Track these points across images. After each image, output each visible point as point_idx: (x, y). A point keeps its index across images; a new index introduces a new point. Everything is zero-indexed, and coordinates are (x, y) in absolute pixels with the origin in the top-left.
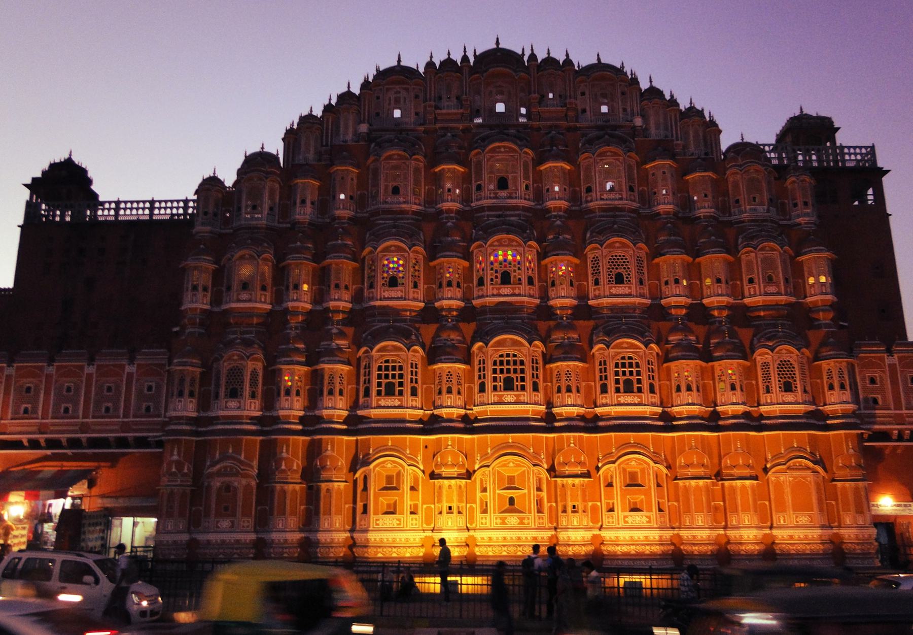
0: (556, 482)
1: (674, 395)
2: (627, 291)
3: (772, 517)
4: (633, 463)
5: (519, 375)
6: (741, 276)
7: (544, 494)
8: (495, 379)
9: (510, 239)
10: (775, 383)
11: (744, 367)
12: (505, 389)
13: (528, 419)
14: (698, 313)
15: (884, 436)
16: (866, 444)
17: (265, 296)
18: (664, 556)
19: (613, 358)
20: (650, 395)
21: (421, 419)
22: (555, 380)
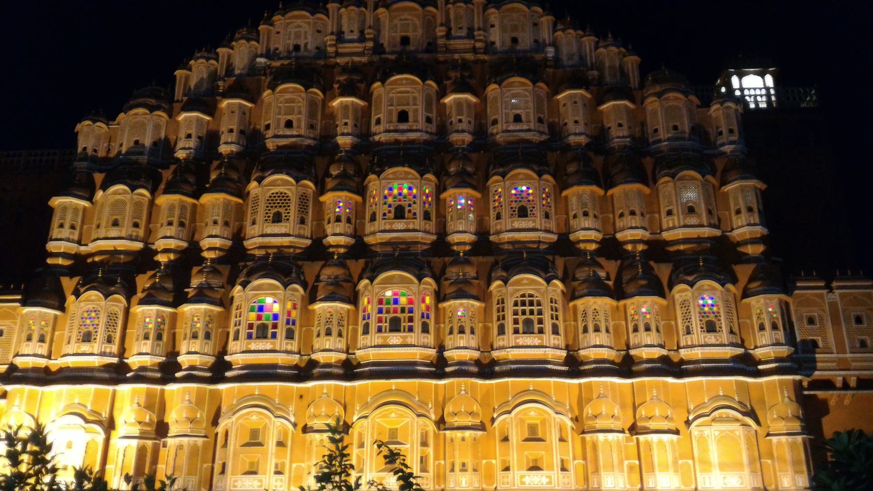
0: (445, 434)
1: (581, 336)
2: (531, 225)
3: (696, 479)
4: (532, 413)
5: (407, 315)
6: (659, 208)
7: (430, 450)
8: (380, 320)
9: (405, 172)
10: (696, 324)
11: (661, 306)
12: (391, 331)
13: (415, 364)
14: (611, 247)
15: (828, 385)
16: (806, 393)
17: (137, 232)
19: (512, 295)
20: (552, 336)
21: (296, 365)
22: (447, 321)
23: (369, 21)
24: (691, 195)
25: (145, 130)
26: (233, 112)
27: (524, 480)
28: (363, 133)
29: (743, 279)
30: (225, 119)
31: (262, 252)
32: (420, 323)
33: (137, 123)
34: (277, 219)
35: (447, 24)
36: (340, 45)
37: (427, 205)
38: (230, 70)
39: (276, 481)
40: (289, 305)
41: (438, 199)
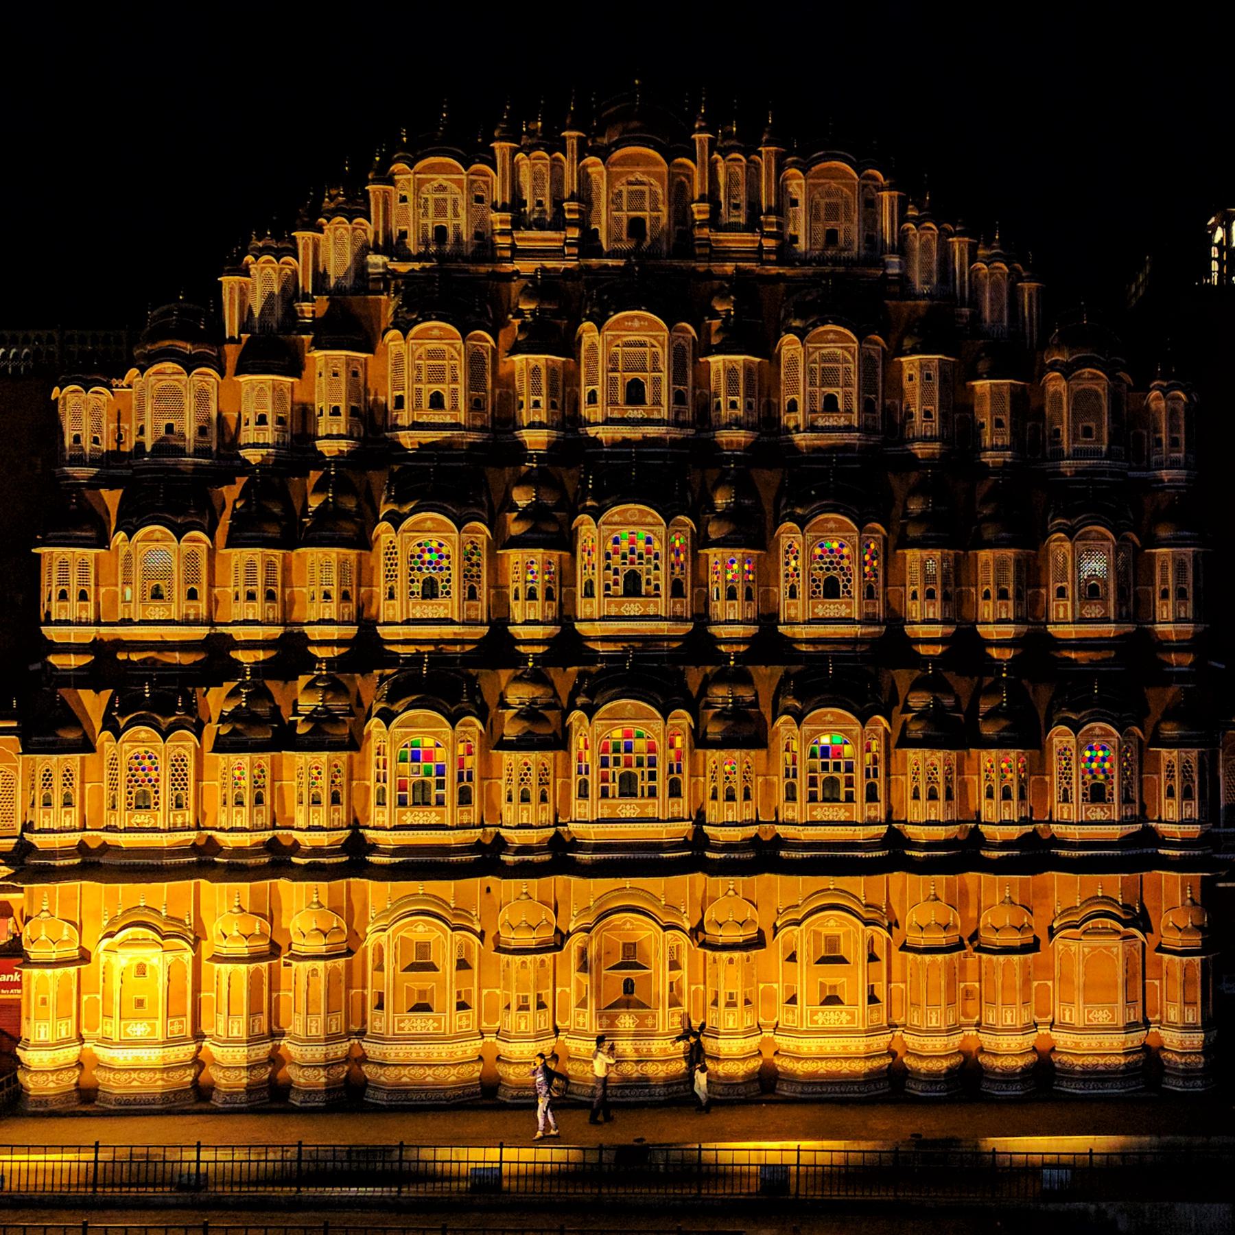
4: (832, 923)
9: (640, 511)
18: (872, 1077)
23: (570, 184)
24: (1096, 566)
25: (182, 404)
26: (335, 374)
27: (815, 1018)
28: (567, 419)
29: (1156, 712)
30: (322, 383)
31: (411, 649)
32: (667, 783)
33: (164, 389)
35: (711, 197)
37: (677, 569)
38: (320, 278)
39: (460, 1019)
40: (461, 749)
41: (695, 557)
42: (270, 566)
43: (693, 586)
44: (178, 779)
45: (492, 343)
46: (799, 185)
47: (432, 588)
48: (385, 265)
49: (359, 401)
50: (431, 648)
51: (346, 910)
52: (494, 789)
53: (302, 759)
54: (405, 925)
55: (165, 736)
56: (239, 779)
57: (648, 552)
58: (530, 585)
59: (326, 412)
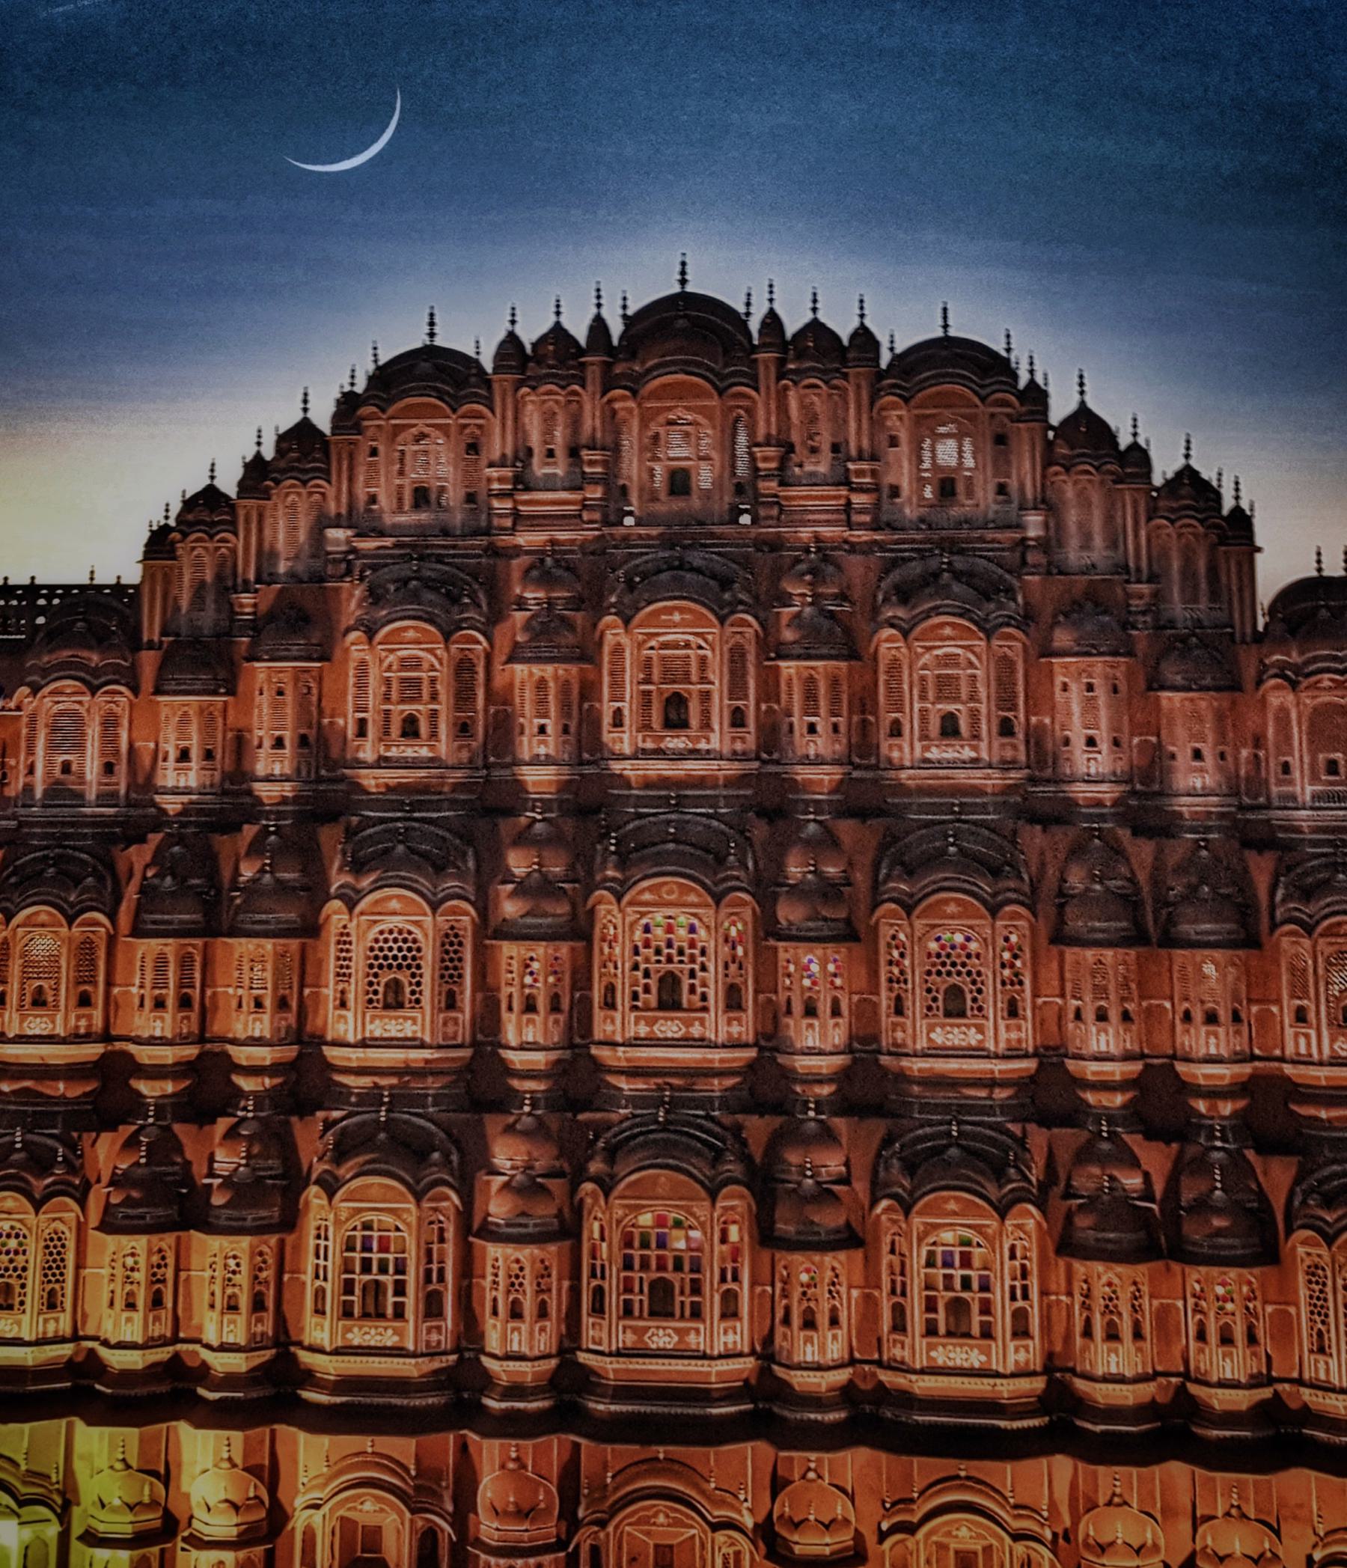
34: (394, 1000)
36: (526, 497)
37: (733, 967)
42: (185, 962)
43: (756, 992)
44: (53, 1268)
45: (485, 644)
46: (900, 418)
47: (396, 993)
48: (348, 541)
49: (310, 727)
50: (394, 1081)
51: (268, 1473)
52: (475, 1292)
53: (216, 1243)
54: (347, 1500)
55: (38, 1205)
56: (132, 1269)
57: (692, 945)
58: (527, 991)
59: (267, 743)
